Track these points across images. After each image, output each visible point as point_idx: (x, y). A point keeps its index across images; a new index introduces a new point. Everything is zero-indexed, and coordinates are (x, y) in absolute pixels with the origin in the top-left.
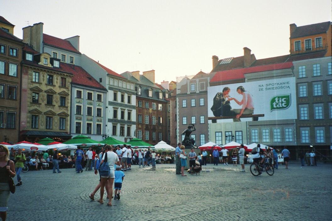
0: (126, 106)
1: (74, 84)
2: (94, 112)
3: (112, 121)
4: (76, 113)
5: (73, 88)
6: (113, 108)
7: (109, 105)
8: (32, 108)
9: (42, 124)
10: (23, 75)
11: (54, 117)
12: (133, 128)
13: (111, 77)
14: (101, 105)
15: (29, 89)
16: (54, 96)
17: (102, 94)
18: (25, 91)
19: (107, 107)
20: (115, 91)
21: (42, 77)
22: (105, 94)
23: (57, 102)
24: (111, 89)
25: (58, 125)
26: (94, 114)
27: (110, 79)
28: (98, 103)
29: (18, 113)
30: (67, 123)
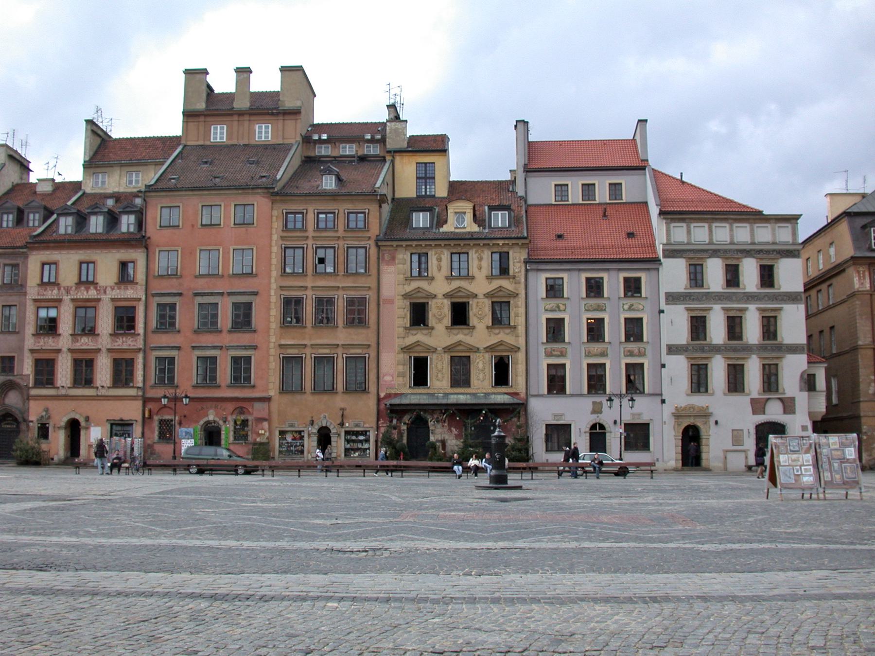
0: (751, 297)
1: (534, 262)
2: (614, 331)
4: (545, 341)
5: (530, 274)
6: (688, 309)
7: (667, 304)
8: (411, 340)
9: (440, 375)
10: (384, 268)
12: (793, 367)
14: (641, 307)
15: (400, 297)
16: (473, 303)
17: (643, 276)
18: (391, 302)
19: (663, 311)
20: (690, 258)
21: (435, 262)
22: (654, 273)
23: (480, 319)
24: (672, 253)
28: (629, 301)
29: (373, 354)
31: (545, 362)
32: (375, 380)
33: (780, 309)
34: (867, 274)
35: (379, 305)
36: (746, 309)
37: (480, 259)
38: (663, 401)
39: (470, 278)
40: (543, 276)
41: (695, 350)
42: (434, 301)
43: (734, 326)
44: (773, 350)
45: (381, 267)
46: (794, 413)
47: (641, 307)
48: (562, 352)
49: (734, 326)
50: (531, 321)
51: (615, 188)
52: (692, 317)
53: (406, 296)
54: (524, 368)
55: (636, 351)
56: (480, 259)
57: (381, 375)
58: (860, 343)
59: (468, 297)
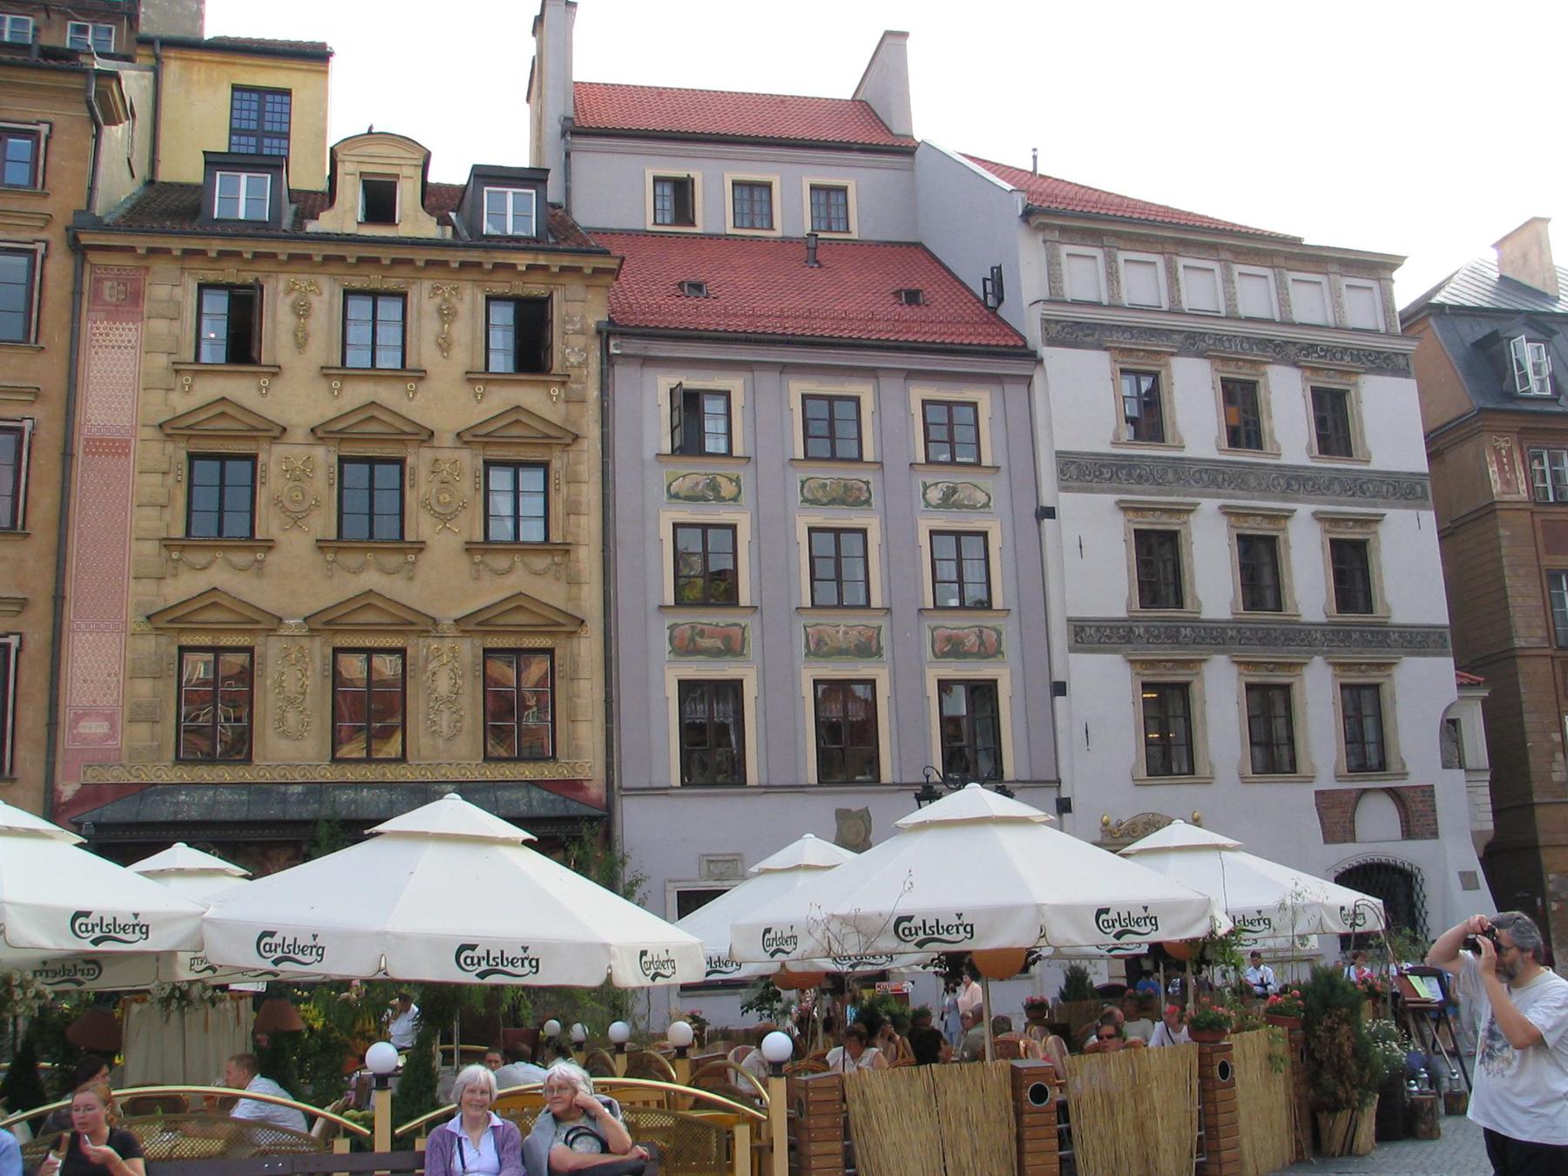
0: (1296, 481)
3: (1129, 641)
4: (670, 599)
5: (624, 377)
6: (1125, 507)
8: (184, 586)
9: (292, 717)
10: (96, 328)
11: (418, 648)
13: (1063, 230)
14: (982, 498)
15: (149, 433)
16: (418, 460)
17: (983, 397)
18: (117, 447)
19: (1050, 513)
22: (1015, 392)
23: (444, 518)
25: (467, 723)
26: (889, 593)
27: (1065, 249)
29: (37, 639)
30: (571, 698)
31: (674, 673)
32: (42, 733)
33: (1376, 520)
34: (1517, 456)
35: (67, 455)
36: (1286, 516)
37: (447, 315)
38: (1064, 806)
39: (409, 374)
40: (663, 383)
41: (1153, 638)
42: (279, 450)
43: (1259, 560)
44: (1366, 644)
45: (87, 325)
46: (1435, 834)
47: (982, 498)
48: (727, 639)
49: (1259, 560)
50: (624, 529)
51: (829, 197)
52: (1139, 534)
53: (170, 429)
54: (599, 694)
55: (971, 641)
56: (447, 315)
57: (66, 716)
58: (1518, 643)
59: (401, 438)
